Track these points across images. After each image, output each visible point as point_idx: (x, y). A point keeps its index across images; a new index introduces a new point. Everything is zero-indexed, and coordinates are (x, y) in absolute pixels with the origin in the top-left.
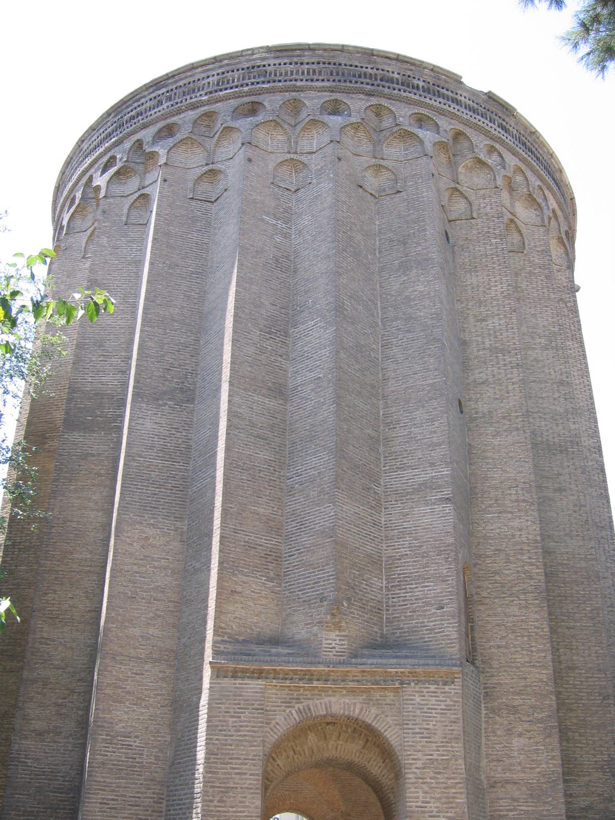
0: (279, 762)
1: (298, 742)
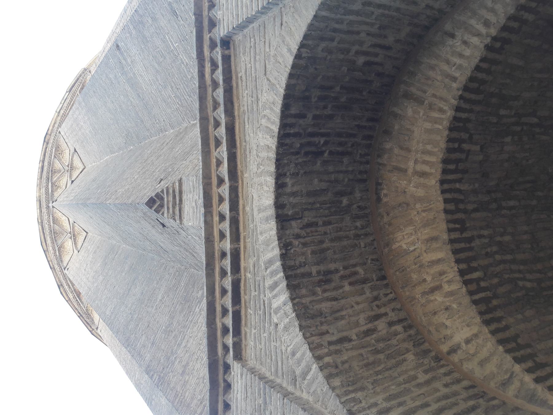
1: (415, 276)
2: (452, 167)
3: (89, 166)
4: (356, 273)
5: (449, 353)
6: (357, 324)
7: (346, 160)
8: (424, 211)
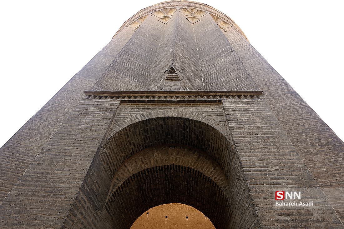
0: (129, 168)
2: (178, 168)
3: (193, 26)
4: (147, 139)
5: (125, 165)
6: (132, 140)
7: (182, 137)
8: (165, 160)
